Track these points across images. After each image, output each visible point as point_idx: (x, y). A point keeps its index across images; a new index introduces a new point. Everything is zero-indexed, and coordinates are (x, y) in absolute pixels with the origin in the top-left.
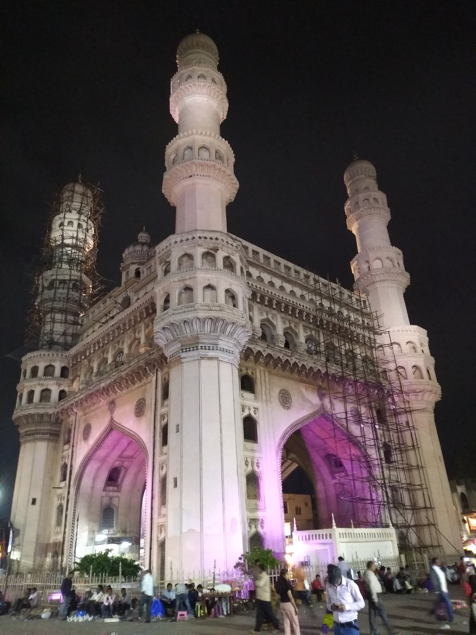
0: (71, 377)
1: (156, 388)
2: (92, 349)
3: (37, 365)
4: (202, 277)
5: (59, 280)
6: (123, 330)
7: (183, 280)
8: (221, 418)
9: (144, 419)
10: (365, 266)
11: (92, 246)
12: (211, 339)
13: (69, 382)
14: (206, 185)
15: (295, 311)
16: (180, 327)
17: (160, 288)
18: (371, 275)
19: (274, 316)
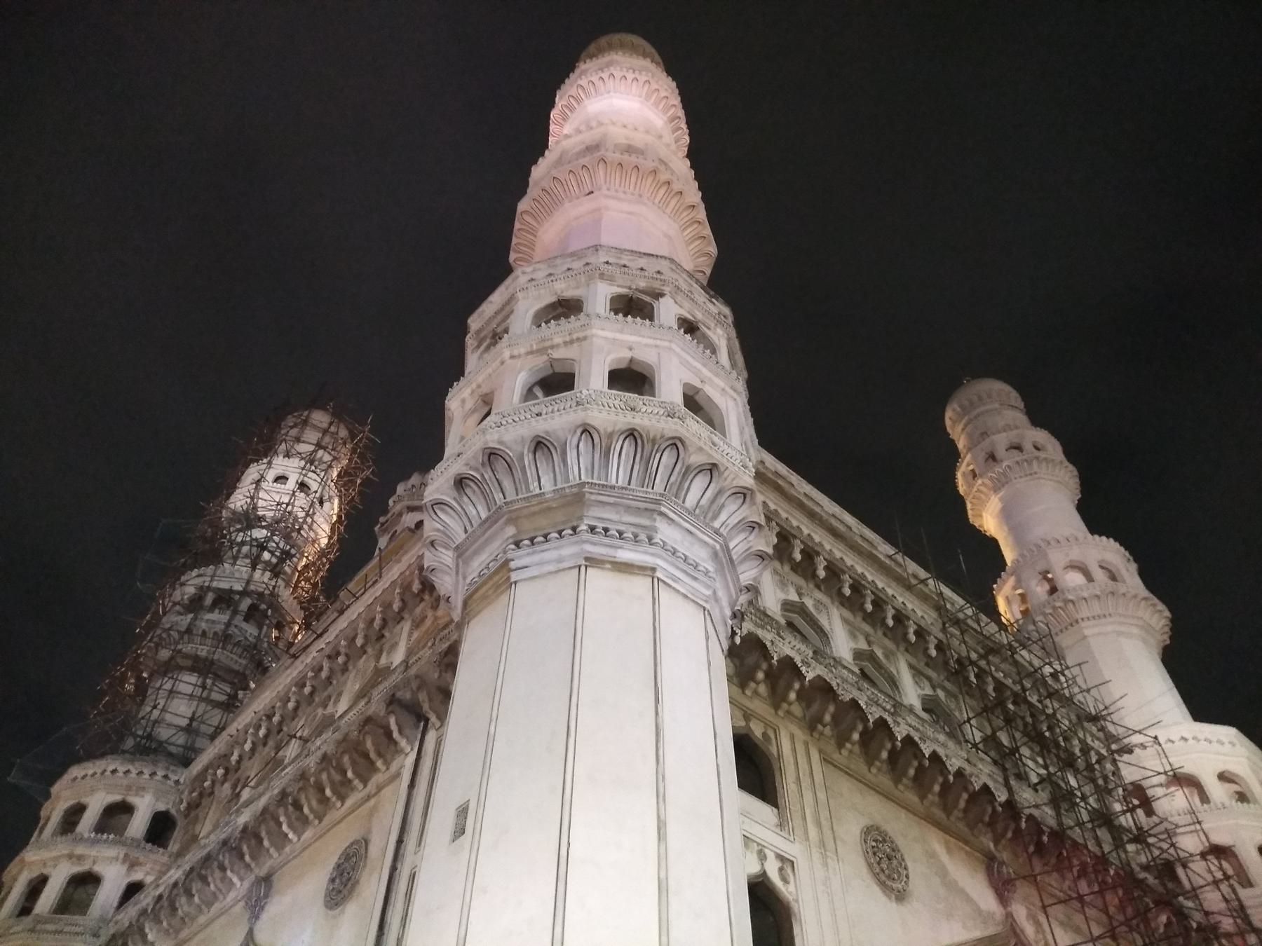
0: (174, 846)
1: (412, 785)
2: (249, 741)
3: (84, 800)
4: (607, 341)
6: (347, 655)
7: (541, 351)
8: (660, 777)
9: (351, 908)
11: (324, 542)
12: (628, 509)
13: (165, 859)
14: (630, 213)
15: (884, 611)
16: (518, 474)
17: (466, 393)
18: (1067, 601)
19: (821, 607)
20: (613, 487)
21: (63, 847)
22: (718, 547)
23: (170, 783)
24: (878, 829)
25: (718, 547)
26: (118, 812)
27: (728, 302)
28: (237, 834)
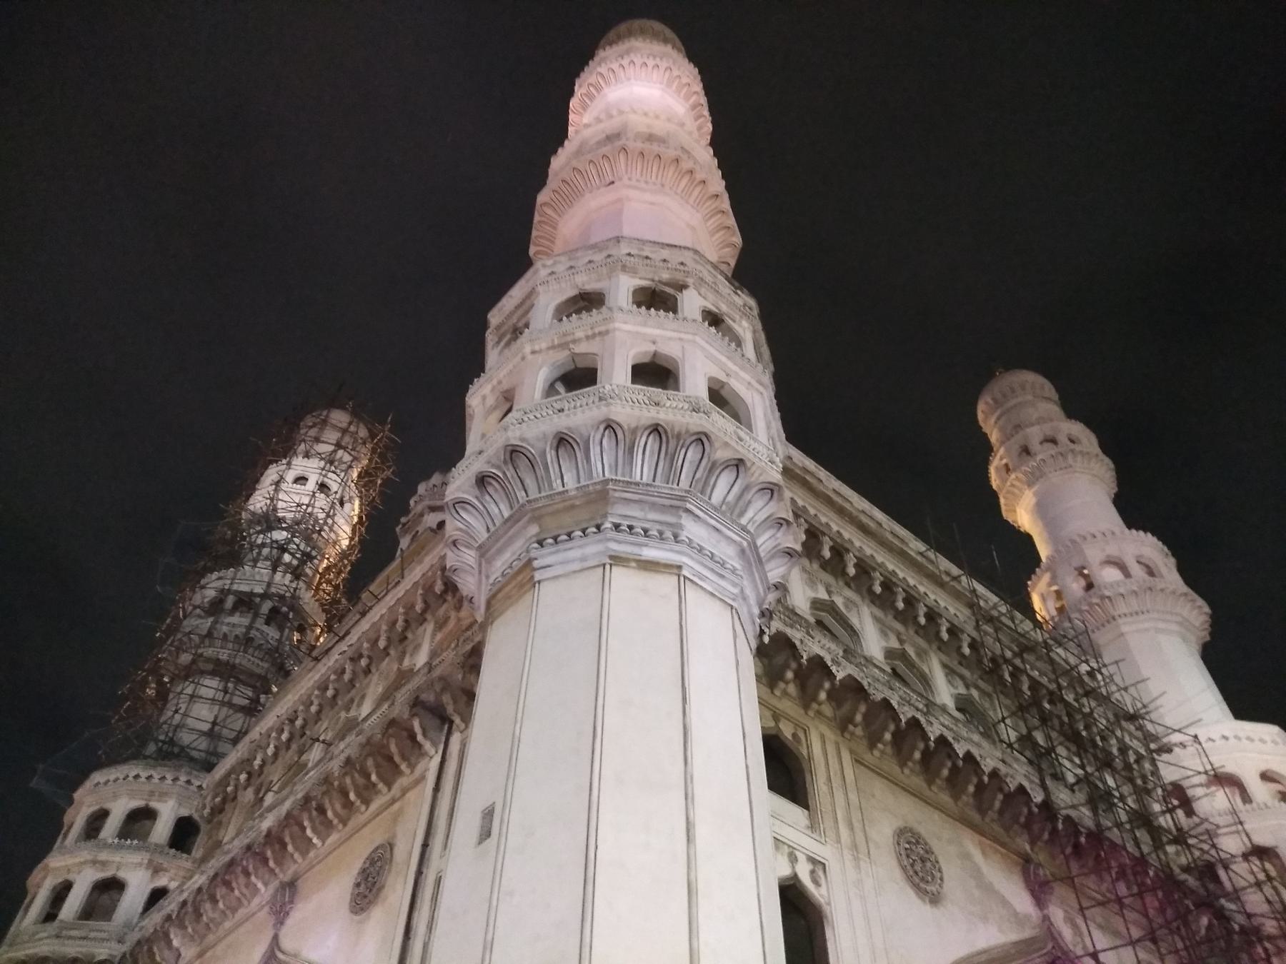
0: (198, 852)
1: (437, 789)
2: (272, 746)
3: (107, 806)
4: (630, 335)
5: (237, 593)
6: (369, 657)
7: (563, 346)
8: (688, 779)
9: (377, 914)
10: (1075, 587)
11: (345, 543)
12: (654, 506)
14: (652, 204)
16: (541, 471)
18: (1103, 597)
19: (851, 605)
20: (637, 484)
21: (85, 854)
22: (745, 544)
23: (193, 788)
24: (911, 830)
25: (745, 544)
26: (141, 818)
27: (753, 293)
28: (261, 840)
